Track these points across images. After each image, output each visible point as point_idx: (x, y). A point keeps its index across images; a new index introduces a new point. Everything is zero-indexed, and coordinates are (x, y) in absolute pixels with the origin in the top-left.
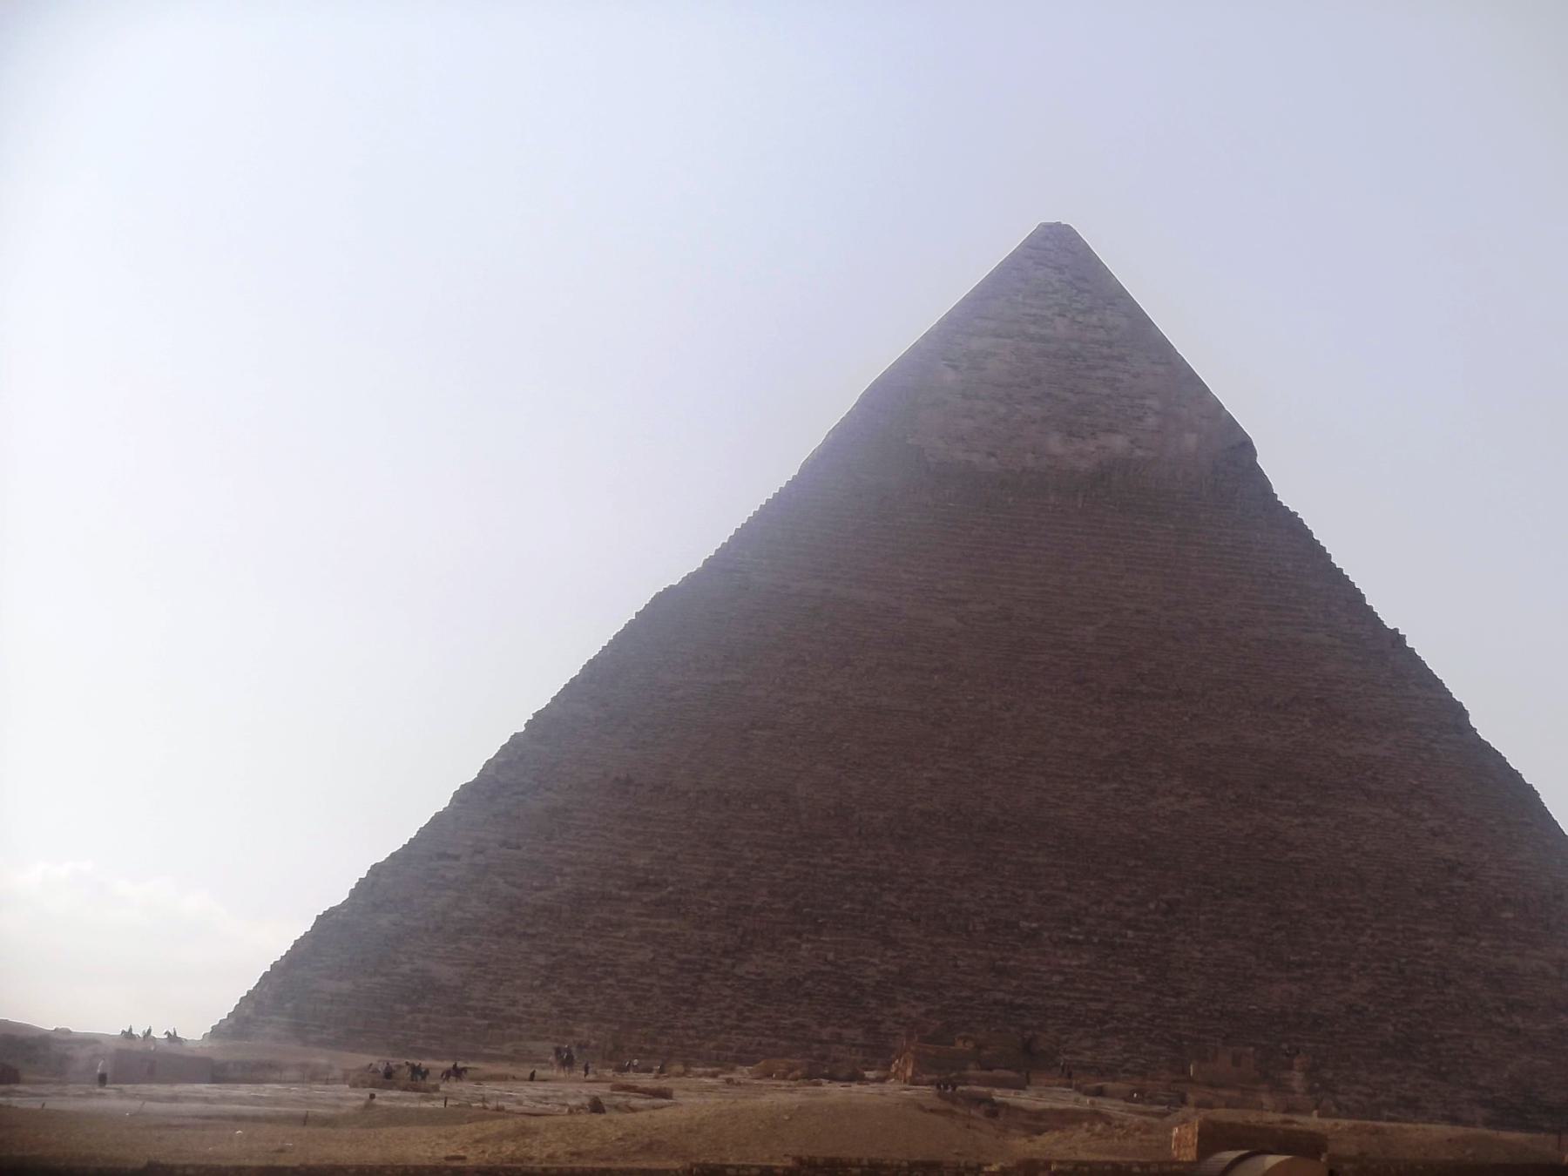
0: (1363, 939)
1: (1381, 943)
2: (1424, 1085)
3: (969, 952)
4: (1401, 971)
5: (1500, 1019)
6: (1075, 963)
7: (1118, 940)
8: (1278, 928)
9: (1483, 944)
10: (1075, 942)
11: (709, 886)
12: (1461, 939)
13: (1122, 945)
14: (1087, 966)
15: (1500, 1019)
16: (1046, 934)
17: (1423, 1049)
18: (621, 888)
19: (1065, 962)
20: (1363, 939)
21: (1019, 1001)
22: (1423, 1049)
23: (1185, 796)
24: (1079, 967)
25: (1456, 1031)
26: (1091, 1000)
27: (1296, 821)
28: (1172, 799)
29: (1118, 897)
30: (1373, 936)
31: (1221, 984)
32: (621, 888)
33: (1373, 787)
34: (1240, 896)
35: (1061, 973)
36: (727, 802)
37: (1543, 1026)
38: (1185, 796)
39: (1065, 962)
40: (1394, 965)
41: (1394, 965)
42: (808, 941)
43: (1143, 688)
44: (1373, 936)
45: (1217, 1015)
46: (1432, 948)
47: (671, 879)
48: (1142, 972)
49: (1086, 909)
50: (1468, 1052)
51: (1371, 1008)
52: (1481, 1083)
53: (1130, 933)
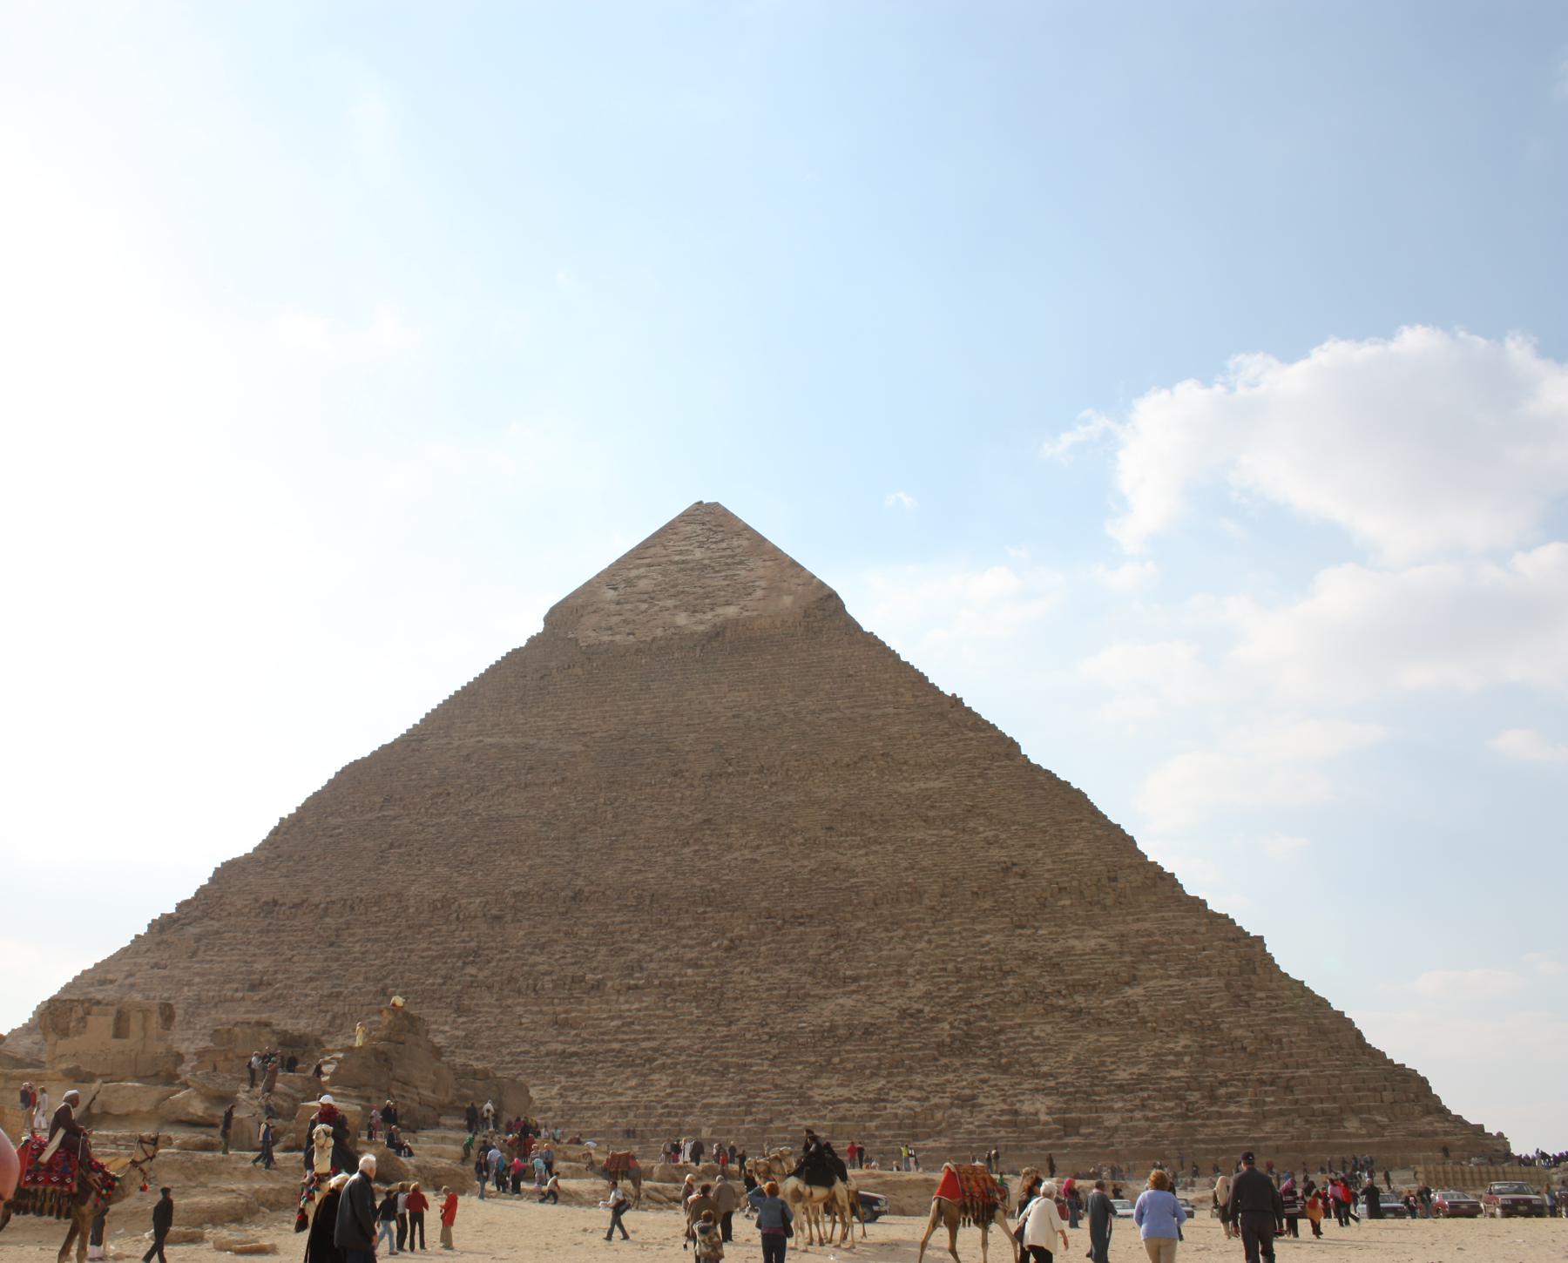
0: (919, 946)
1: (938, 947)
2: (984, 1081)
3: (535, 1009)
4: (958, 970)
5: (1061, 1002)
6: (636, 1006)
7: (677, 979)
8: (836, 948)
10: (636, 987)
11: (311, 979)
13: (680, 984)
14: (646, 1008)
15: (1061, 1002)
16: (610, 984)
17: (983, 1043)
18: (237, 990)
19: (626, 1006)
20: (919, 946)
21: (573, 1049)
22: (983, 1043)
24: (639, 1010)
25: (1018, 1021)
26: (644, 1040)
28: (746, 852)
29: (685, 941)
30: (930, 941)
31: (773, 1007)
32: (237, 990)
35: (620, 1017)
36: (352, 908)
37: (1107, 1002)
39: (626, 1006)
40: (950, 966)
41: (950, 966)
44: (930, 941)
45: (766, 1037)
47: (280, 976)
48: (698, 1007)
49: (651, 955)
50: (1030, 1040)
51: (927, 1009)
52: (1045, 1069)
53: (690, 972)
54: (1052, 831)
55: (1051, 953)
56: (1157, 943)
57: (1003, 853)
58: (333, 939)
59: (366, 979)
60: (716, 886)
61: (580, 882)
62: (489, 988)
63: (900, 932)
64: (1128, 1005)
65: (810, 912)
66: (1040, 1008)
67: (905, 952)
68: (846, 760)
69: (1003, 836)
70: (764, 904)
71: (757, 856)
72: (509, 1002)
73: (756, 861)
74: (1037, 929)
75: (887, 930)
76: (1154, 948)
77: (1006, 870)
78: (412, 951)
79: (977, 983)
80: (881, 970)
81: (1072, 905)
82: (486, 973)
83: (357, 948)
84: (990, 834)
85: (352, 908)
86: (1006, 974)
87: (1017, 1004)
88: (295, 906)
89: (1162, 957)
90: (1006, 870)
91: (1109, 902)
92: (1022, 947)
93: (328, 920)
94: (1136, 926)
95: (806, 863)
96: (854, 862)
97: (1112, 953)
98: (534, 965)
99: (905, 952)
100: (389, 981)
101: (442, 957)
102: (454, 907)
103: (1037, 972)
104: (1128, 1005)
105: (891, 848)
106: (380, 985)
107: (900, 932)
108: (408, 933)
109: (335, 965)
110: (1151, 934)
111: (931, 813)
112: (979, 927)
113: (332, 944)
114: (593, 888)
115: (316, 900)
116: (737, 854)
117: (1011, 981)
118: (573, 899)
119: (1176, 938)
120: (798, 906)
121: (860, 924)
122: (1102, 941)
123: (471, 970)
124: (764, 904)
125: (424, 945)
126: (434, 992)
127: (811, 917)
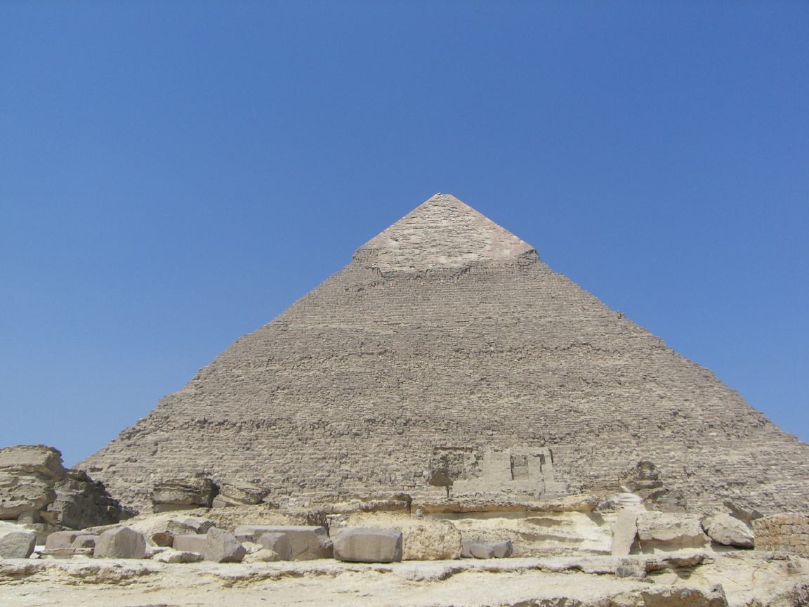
5: (725, 493)
8: (581, 458)
9: (703, 451)
12: (690, 450)
23: (518, 396)
27: (583, 401)
28: (512, 398)
30: (637, 455)
33: (622, 379)
34: (555, 443)
37: (752, 493)
38: (518, 396)
42: (294, 496)
43: (492, 349)
44: (637, 455)
46: (674, 457)
54: (698, 391)
55: (714, 463)
56: (773, 459)
57: (671, 403)
58: (248, 446)
59: (275, 471)
60: (497, 418)
61: (408, 414)
62: (360, 479)
63: (617, 449)
64: (766, 495)
65: (561, 436)
66: (712, 496)
67: (624, 461)
68: (563, 346)
69: (669, 394)
70: (531, 430)
71: (519, 400)
72: (374, 488)
73: (520, 405)
74: (701, 449)
75: (609, 448)
76: (773, 462)
77: (675, 414)
78: (304, 454)
79: (671, 480)
80: (612, 471)
81: (717, 436)
82: (358, 469)
83: (265, 451)
84: (661, 392)
85: (258, 427)
86: (689, 475)
87: (698, 494)
88: (220, 424)
89: (778, 467)
90: (675, 414)
91: (740, 434)
92: (696, 459)
93: (242, 433)
94: (760, 449)
95: (550, 406)
96: (581, 407)
97: (751, 465)
98: (388, 465)
99: (624, 461)
100: (291, 473)
101: (324, 458)
102: (328, 427)
103: (708, 475)
104: (766, 495)
105: (603, 399)
106: (286, 476)
107: (617, 449)
108: (300, 443)
109: (252, 462)
110: (769, 454)
111: (622, 379)
112: (666, 447)
113: (248, 449)
114: (418, 418)
115: (234, 421)
116: (506, 400)
117: (692, 480)
118: (405, 424)
119: (786, 457)
120: (552, 432)
121: (592, 444)
122: (743, 457)
123: (344, 467)
124: (531, 430)
125: (311, 451)
126: (324, 480)
127: (561, 439)
